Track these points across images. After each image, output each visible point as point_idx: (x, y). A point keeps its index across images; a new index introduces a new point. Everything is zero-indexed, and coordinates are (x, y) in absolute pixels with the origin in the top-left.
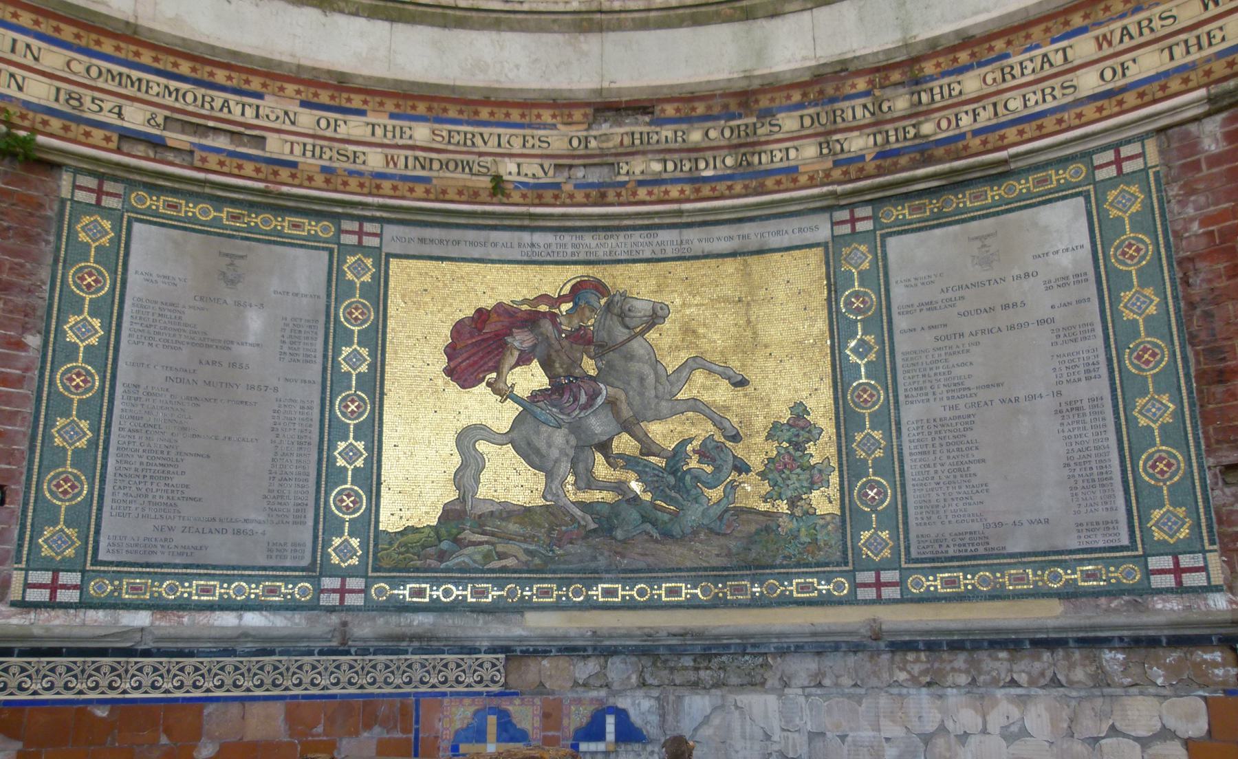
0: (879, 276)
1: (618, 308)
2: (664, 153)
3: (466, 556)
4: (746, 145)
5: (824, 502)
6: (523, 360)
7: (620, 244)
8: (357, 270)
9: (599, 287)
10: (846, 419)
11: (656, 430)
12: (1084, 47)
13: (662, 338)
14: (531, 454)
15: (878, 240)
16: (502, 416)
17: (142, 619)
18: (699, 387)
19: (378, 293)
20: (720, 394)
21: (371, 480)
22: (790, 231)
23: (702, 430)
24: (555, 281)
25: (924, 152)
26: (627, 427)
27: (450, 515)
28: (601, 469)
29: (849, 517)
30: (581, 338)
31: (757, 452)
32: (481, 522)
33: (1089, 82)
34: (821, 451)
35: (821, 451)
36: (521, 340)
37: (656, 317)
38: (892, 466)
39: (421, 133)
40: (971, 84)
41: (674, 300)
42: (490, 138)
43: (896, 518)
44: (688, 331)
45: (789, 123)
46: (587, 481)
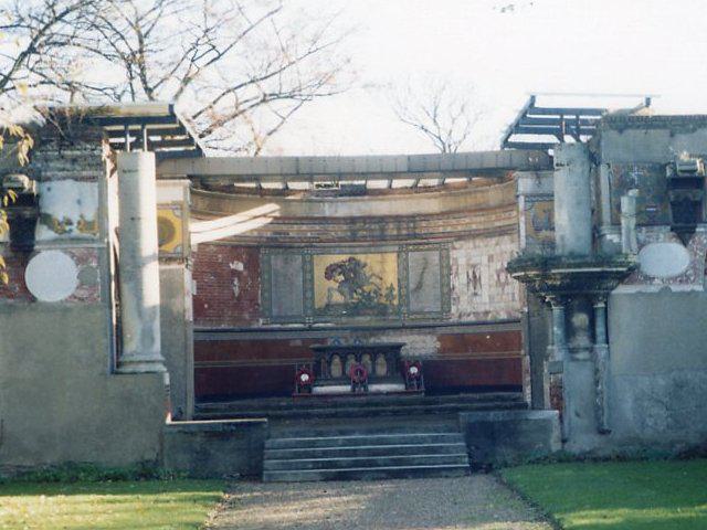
0: (406, 259)
1: (358, 263)
2: (366, 230)
3: (329, 313)
4: (383, 230)
5: (396, 302)
6: (340, 274)
7: (357, 250)
8: (308, 258)
9: (354, 259)
10: (400, 287)
11: (365, 288)
12: (441, 223)
13: (366, 269)
14: (342, 293)
15: (407, 252)
16: (336, 285)
17: (278, 326)
18: (373, 279)
19: (311, 262)
20: (378, 280)
21: (312, 298)
22: (390, 248)
23: (373, 287)
24: (344, 257)
25: (415, 236)
26: (360, 287)
27: (327, 305)
28: (355, 295)
29: (400, 305)
30: (350, 270)
31: (384, 292)
32: (333, 306)
33: (441, 229)
34: (395, 293)
35: (395, 293)
36: (340, 270)
37: (365, 265)
38: (407, 296)
39: (317, 227)
40: (424, 224)
41: (368, 261)
42: (330, 227)
43: (408, 305)
44: (371, 268)
45: (391, 226)
46: (352, 298)
